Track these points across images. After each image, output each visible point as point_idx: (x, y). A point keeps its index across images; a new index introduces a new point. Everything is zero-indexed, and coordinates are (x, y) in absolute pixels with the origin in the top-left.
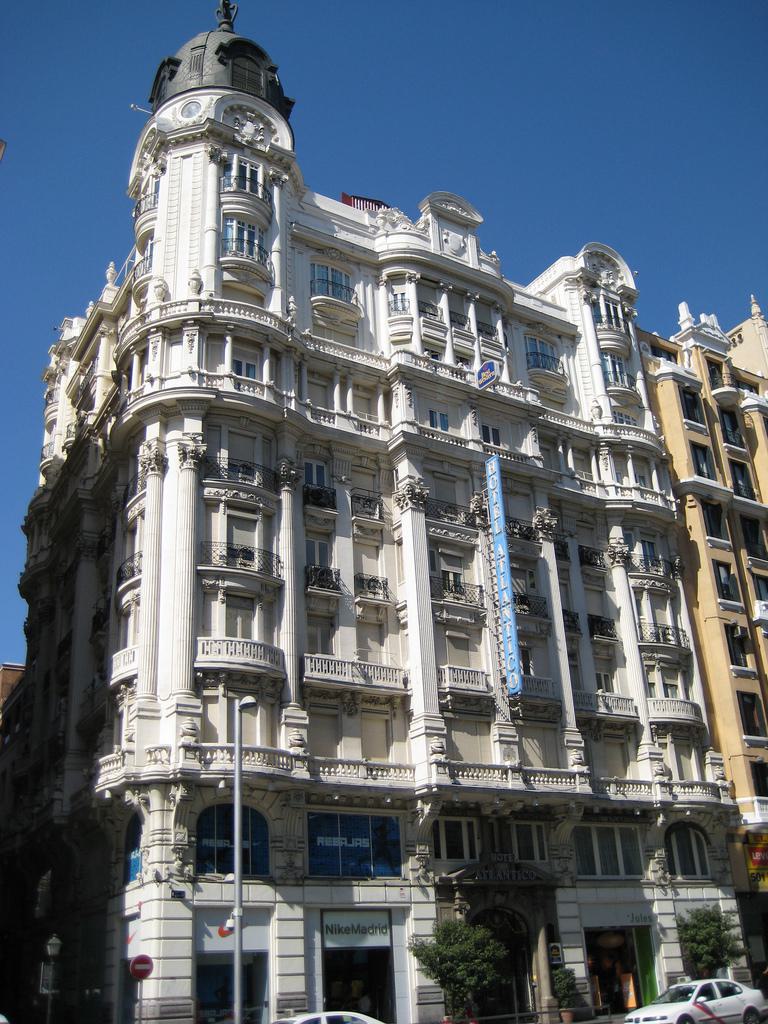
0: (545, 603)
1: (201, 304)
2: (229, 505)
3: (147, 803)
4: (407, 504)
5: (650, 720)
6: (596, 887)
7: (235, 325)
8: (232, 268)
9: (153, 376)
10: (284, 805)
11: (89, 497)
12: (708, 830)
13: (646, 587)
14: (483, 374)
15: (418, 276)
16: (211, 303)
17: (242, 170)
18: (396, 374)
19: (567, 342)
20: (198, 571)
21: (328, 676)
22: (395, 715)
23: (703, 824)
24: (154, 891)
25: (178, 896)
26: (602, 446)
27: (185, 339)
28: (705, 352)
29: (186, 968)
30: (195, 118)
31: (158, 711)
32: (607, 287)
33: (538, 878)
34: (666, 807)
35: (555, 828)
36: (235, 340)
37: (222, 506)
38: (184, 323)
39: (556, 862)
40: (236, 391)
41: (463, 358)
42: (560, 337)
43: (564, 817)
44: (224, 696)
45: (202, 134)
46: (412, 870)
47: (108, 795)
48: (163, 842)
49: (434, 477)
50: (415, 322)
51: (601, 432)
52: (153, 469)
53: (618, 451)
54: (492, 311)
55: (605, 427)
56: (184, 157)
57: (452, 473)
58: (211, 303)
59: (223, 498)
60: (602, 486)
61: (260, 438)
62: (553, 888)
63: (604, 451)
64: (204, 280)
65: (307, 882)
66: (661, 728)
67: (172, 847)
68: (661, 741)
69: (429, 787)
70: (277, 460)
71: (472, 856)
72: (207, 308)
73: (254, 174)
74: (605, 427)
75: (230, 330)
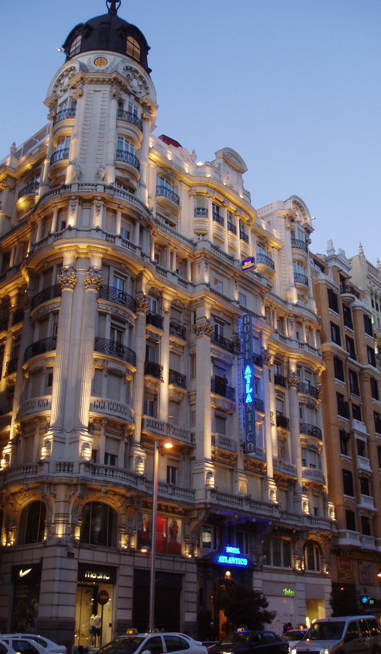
0: (263, 404)
1: (105, 187)
2: (113, 317)
10: (129, 506)
14: (246, 264)
17: (130, 107)
27: (95, 208)
30: (103, 68)
31: (64, 439)
32: (298, 222)
37: (108, 316)
38: (94, 198)
40: (122, 247)
44: (104, 435)
45: (110, 80)
56: (95, 91)
69: (206, 504)
70: (136, 293)
71: (215, 548)
73: (136, 112)
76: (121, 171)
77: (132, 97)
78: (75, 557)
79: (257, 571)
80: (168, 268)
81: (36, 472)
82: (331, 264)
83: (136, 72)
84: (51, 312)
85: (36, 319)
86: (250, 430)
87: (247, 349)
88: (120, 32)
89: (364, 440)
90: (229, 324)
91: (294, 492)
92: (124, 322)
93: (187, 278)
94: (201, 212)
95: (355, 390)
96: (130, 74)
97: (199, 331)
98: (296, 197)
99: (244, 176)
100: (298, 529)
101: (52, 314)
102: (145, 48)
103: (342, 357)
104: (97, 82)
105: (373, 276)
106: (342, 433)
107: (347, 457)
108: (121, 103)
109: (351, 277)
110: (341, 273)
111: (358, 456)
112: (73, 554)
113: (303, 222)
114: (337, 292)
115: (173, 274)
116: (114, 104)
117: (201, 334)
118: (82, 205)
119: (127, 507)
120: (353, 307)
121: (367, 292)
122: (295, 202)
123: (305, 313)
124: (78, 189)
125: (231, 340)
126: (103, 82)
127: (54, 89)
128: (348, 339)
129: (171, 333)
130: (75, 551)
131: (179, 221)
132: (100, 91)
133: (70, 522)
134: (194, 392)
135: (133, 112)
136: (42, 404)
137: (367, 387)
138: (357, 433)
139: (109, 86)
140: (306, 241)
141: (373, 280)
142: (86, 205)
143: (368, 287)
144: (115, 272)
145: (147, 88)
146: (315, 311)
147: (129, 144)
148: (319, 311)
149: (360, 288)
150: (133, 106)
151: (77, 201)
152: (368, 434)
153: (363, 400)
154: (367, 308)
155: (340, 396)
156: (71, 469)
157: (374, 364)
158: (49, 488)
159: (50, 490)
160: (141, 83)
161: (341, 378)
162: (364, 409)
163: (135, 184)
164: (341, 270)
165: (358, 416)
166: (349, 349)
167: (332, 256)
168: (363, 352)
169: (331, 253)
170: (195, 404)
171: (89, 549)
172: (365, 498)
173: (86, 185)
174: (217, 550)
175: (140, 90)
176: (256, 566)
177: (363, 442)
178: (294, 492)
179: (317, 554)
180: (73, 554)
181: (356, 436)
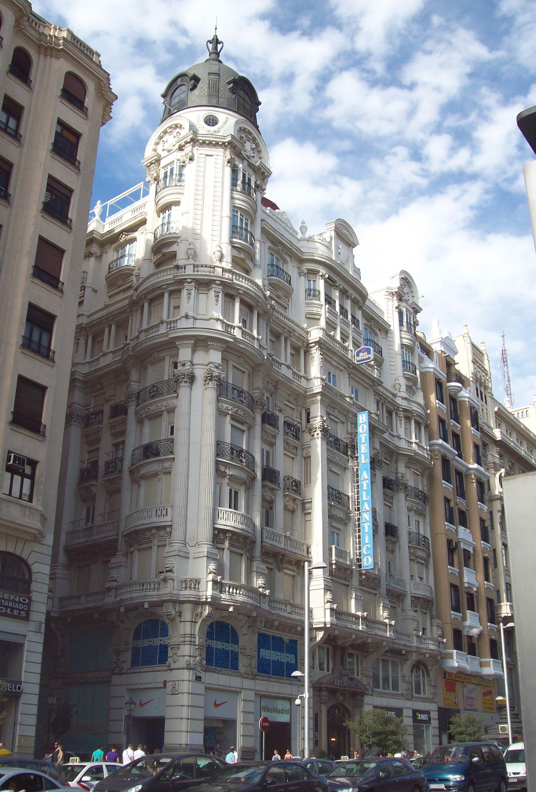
2: (233, 418)
3: (180, 614)
5: (412, 595)
6: (381, 697)
7: (243, 291)
8: (238, 247)
9: (190, 315)
11: (81, 379)
12: (429, 667)
13: (414, 508)
14: (361, 354)
15: (327, 276)
16: (230, 271)
18: (316, 343)
19: (383, 335)
20: (216, 460)
21: (273, 543)
22: (299, 573)
23: (427, 664)
24: (186, 675)
25: (198, 678)
29: (200, 726)
33: (360, 688)
34: (418, 650)
35: (366, 657)
36: (242, 302)
39: (365, 678)
40: (242, 338)
41: (345, 338)
42: (380, 330)
43: (374, 651)
44: (228, 549)
45: (224, 143)
47: (146, 606)
48: (192, 643)
49: (330, 418)
50: (323, 308)
51: (399, 401)
52: (185, 382)
53: (408, 416)
54: (356, 308)
56: (207, 155)
57: (338, 417)
58: (230, 271)
60: (399, 437)
61: (247, 373)
62: (363, 694)
63: (401, 414)
64: (224, 252)
65: (257, 677)
66: (416, 599)
68: (416, 609)
71: (328, 670)
72: (227, 275)
73: (249, 180)
75: (240, 294)
76: (237, 250)
77: (246, 163)
78: (202, 681)
79: (367, 695)
80: (282, 361)
81: (158, 589)
83: (250, 133)
86: (367, 542)
88: (231, 85)
90: (343, 423)
91: (403, 608)
93: (300, 371)
95: (461, 492)
96: (243, 136)
98: (403, 272)
99: (355, 250)
100: (408, 649)
101: (165, 413)
103: (449, 456)
104: (210, 144)
106: (449, 542)
108: (234, 171)
111: (465, 568)
112: (200, 677)
113: (411, 302)
115: (288, 367)
116: (228, 170)
118: (198, 290)
119: (249, 627)
123: (415, 408)
124: (194, 271)
125: (345, 440)
126: (217, 145)
127: (154, 147)
129: (286, 433)
130: (202, 674)
131: (290, 304)
132: (212, 156)
133: (197, 643)
134: (310, 500)
135: (247, 181)
136: (160, 514)
138: (464, 543)
139: (222, 150)
140: (414, 323)
144: (234, 366)
145: (259, 152)
146: (422, 402)
147: (244, 219)
150: (247, 174)
151: (193, 284)
152: (475, 544)
156: (197, 586)
158: (174, 607)
159: (175, 609)
160: (254, 146)
161: (448, 480)
163: (250, 264)
166: (455, 446)
168: (470, 450)
171: (214, 672)
173: (202, 266)
174: (330, 672)
175: (253, 155)
176: (367, 690)
178: (403, 608)
179: (423, 676)
180: (200, 677)
181: (462, 546)
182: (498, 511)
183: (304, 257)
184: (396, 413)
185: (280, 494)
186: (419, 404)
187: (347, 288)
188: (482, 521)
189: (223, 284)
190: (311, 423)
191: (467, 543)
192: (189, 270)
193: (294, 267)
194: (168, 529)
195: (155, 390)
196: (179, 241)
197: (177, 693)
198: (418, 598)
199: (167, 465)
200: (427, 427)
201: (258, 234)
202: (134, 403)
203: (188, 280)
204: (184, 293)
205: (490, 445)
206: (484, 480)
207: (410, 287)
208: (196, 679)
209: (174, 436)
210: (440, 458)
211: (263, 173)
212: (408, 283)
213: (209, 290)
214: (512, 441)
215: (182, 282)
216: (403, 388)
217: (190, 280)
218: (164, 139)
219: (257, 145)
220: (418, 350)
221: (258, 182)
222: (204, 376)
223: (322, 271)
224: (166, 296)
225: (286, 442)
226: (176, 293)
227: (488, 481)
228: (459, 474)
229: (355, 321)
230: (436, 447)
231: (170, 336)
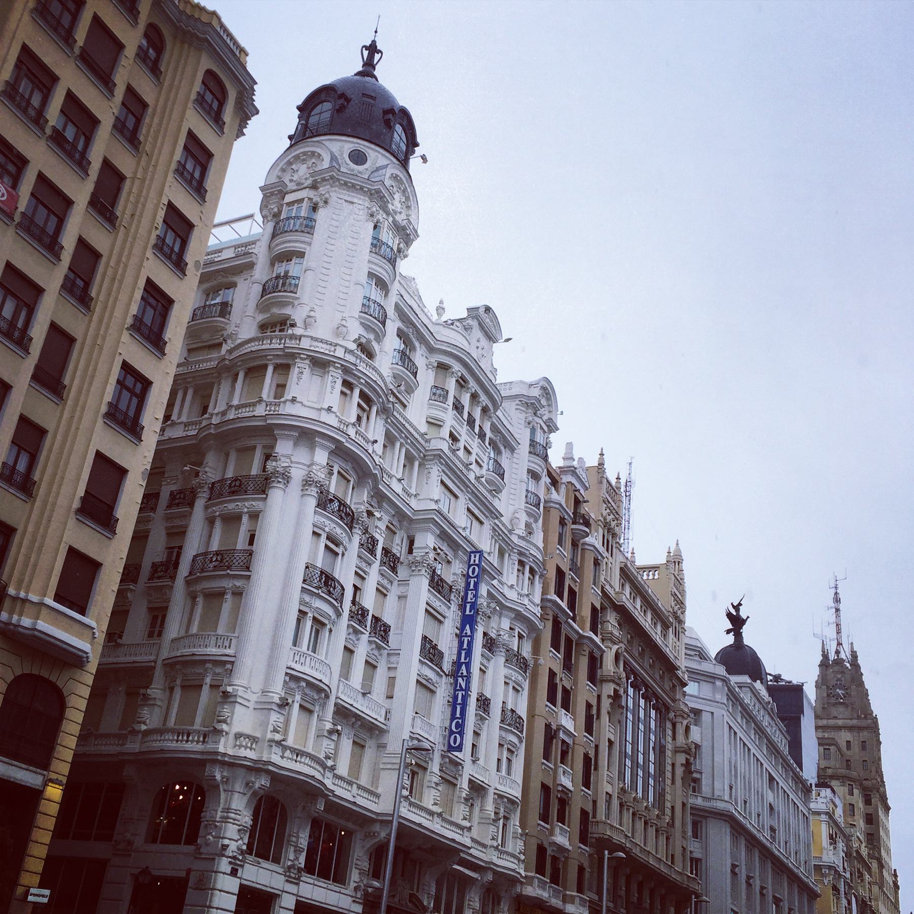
4: (419, 570)
13: (513, 678)
15: (460, 374)
26: (515, 553)
28: (576, 491)
42: (505, 447)
46: (355, 882)
51: (515, 539)
55: (520, 537)
59: (327, 529)
63: (515, 557)
67: (238, 828)
72: (351, 359)
74: (520, 537)
80: (393, 472)
82: (566, 478)
84: (247, 513)
85: (220, 515)
87: (469, 600)
89: (569, 741)
92: (337, 545)
93: (410, 487)
94: (439, 393)
97: (416, 566)
98: (546, 379)
102: (412, 142)
105: (611, 501)
106: (548, 726)
107: (549, 765)
109: (588, 502)
110: (576, 493)
114: (569, 521)
115: (400, 480)
117: (419, 570)
120: (584, 544)
121: (600, 523)
122: (544, 389)
128: (570, 589)
129: (383, 563)
132: (352, 203)
137: (583, 664)
138: (563, 731)
141: (609, 505)
142: (318, 371)
143: (602, 515)
145: (408, 207)
148: (545, 548)
149: (593, 515)
151: (307, 362)
153: (575, 683)
154: (597, 546)
155: (552, 675)
157: (594, 629)
162: (576, 696)
164: (578, 491)
165: (566, 706)
167: (570, 467)
169: (568, 463)
170: (396, 668)
172: (561, 829)
177: (568, 744)
181: (562, 735)
182: (609, 696)
183: (437, 347)
184: (509, 555)
185: (365, 638)
186: (538, 548)
187: (480, 392)
188: (589, 706)
189: (346, 370)
190: (414, 554)
191: (567, 732)
192: (305, 344)
193: (422, 355)
194: (229, 666)
195: (237, 484)
196: (296, 303)
197: (204, 888)
198: (501, 797)
199: (238, 583)
200: (541, 576)
201: (391, 312)
202: (206, 495)
203: (302, 356)
204: (295, 371)
205: (609, 610)
206: (597, 654)
207: (548, 399)
208: (231, 872)
209: (254, 548)
210: (551, 619)
211: (408, 235)
212: (548, 394)
213: (325, 373)
214: (636, 608)
215: (293, 356)
216: (522, 526)
217: (305, 357)
218: (294, 167)
219: (407, 198)
220: (546, 480)
221: (402, 245)
222: (304, 478)
223: (457, 367)
224: (270, 369)
225: (381, 574)
226: (284, 368)
227: (602, 656)
228: (569, 641)
229: (482, 435)
230: (549, 605)
231: (269, 422)
